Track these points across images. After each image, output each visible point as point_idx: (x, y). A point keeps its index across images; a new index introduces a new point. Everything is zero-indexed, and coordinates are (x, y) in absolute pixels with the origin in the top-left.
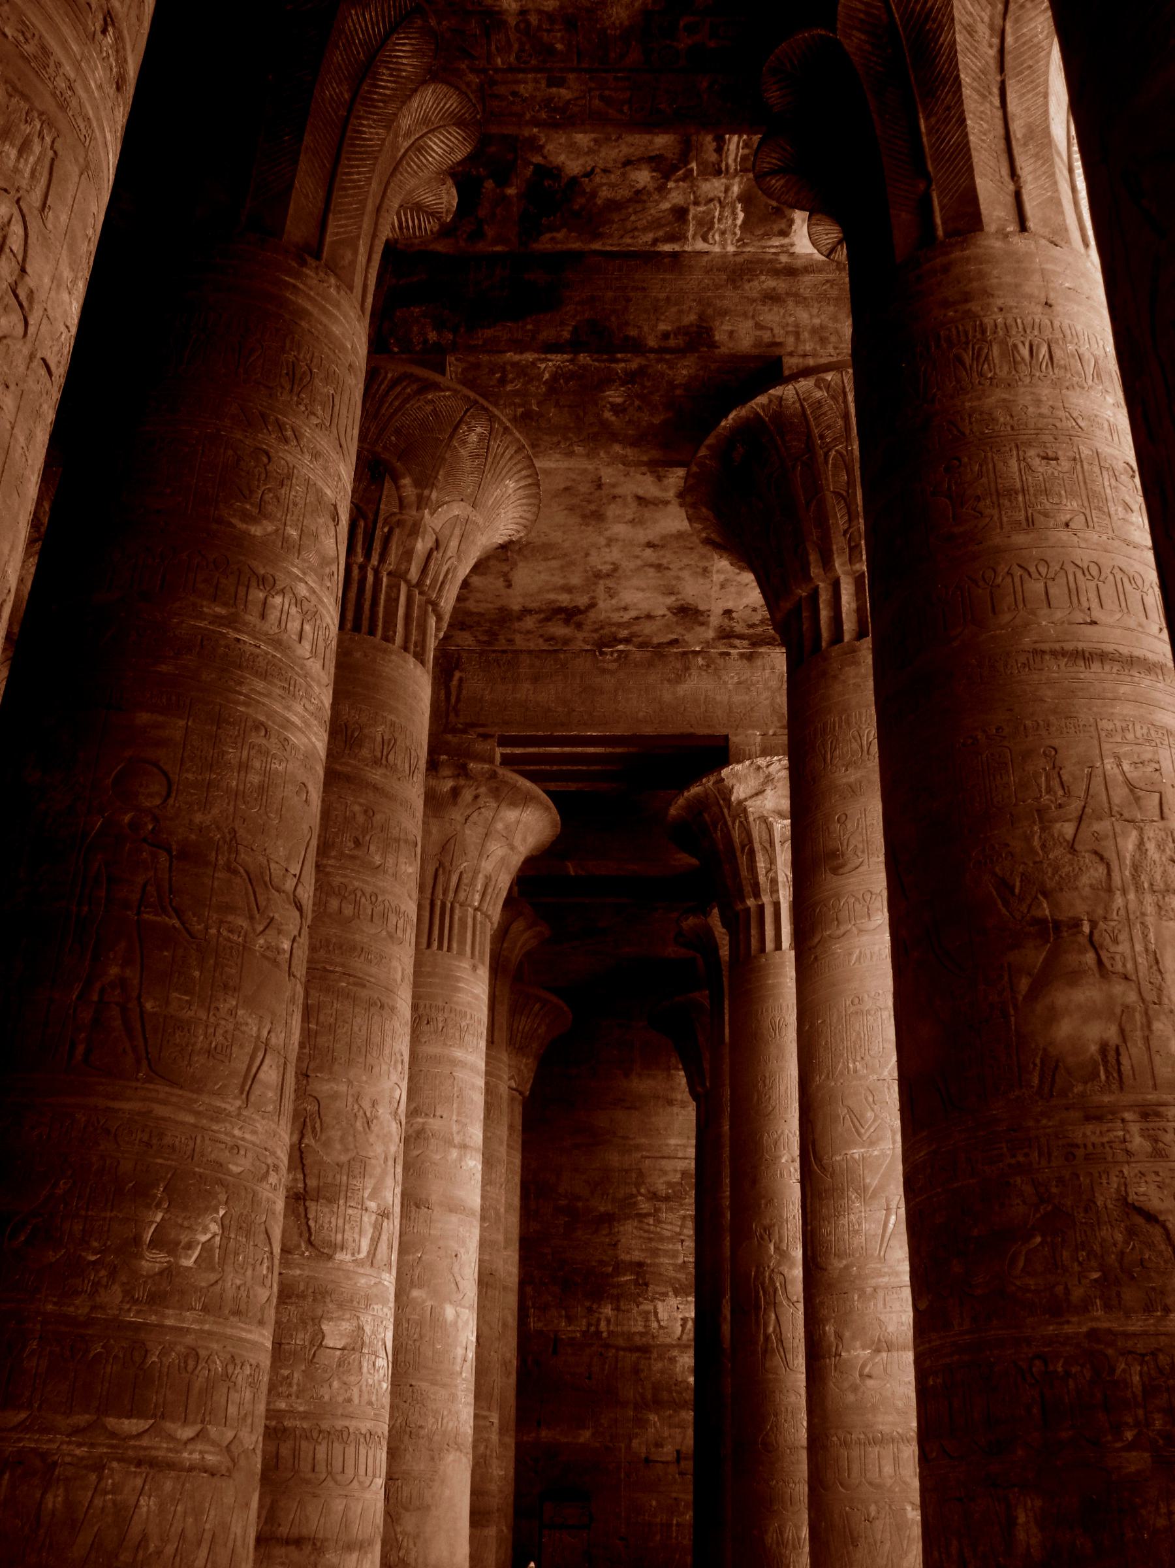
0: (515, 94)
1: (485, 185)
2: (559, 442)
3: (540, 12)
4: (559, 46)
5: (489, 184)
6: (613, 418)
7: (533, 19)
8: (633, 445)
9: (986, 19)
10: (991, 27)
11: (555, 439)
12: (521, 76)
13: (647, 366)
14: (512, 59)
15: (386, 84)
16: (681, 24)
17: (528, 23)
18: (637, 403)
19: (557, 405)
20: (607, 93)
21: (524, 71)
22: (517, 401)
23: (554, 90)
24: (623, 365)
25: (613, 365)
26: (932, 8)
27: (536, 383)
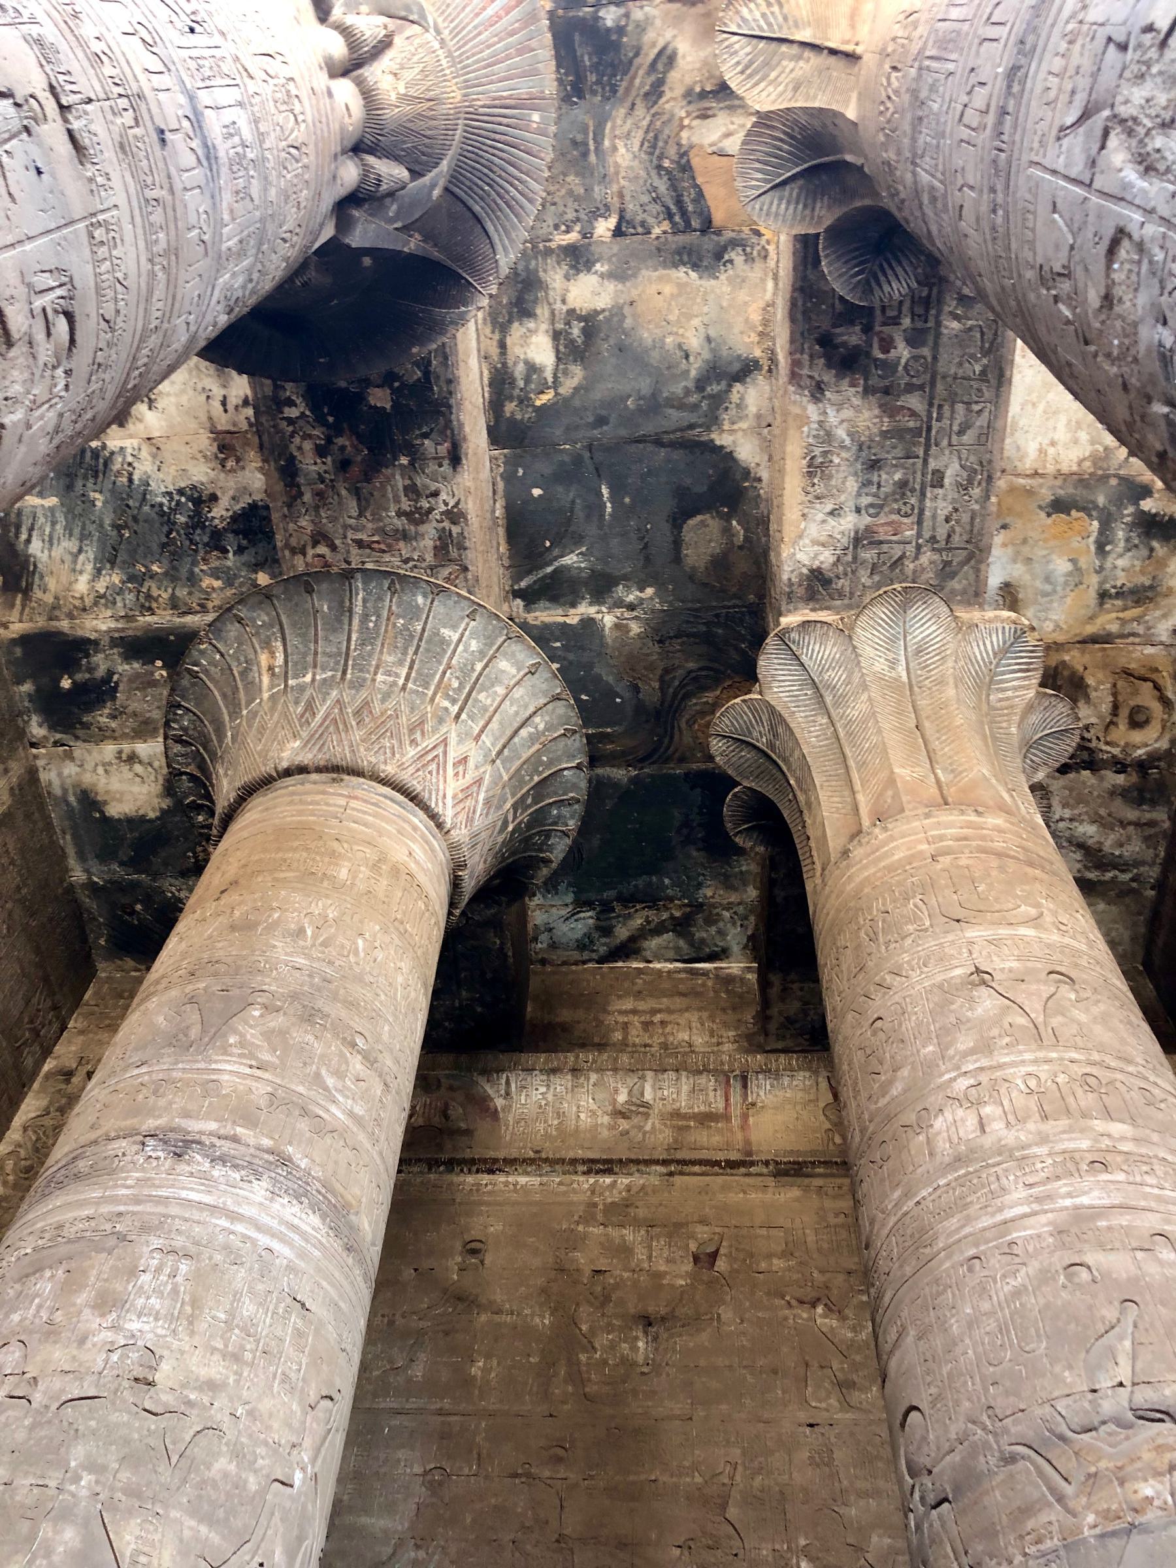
0: (947, 520)
1: (1146, 509)
3: (859, 495)
5: (1147, 505)
7: (865, 501)
9: (792, 65)
10: (799, 58)
12: (927, 513)
14: (905, 520)
15: (835, 676)
16: (881, 356)
17: (871, 505)
20: (956, 428)
21: (922, 511)
23: (947, 481)
26: (785, 133)
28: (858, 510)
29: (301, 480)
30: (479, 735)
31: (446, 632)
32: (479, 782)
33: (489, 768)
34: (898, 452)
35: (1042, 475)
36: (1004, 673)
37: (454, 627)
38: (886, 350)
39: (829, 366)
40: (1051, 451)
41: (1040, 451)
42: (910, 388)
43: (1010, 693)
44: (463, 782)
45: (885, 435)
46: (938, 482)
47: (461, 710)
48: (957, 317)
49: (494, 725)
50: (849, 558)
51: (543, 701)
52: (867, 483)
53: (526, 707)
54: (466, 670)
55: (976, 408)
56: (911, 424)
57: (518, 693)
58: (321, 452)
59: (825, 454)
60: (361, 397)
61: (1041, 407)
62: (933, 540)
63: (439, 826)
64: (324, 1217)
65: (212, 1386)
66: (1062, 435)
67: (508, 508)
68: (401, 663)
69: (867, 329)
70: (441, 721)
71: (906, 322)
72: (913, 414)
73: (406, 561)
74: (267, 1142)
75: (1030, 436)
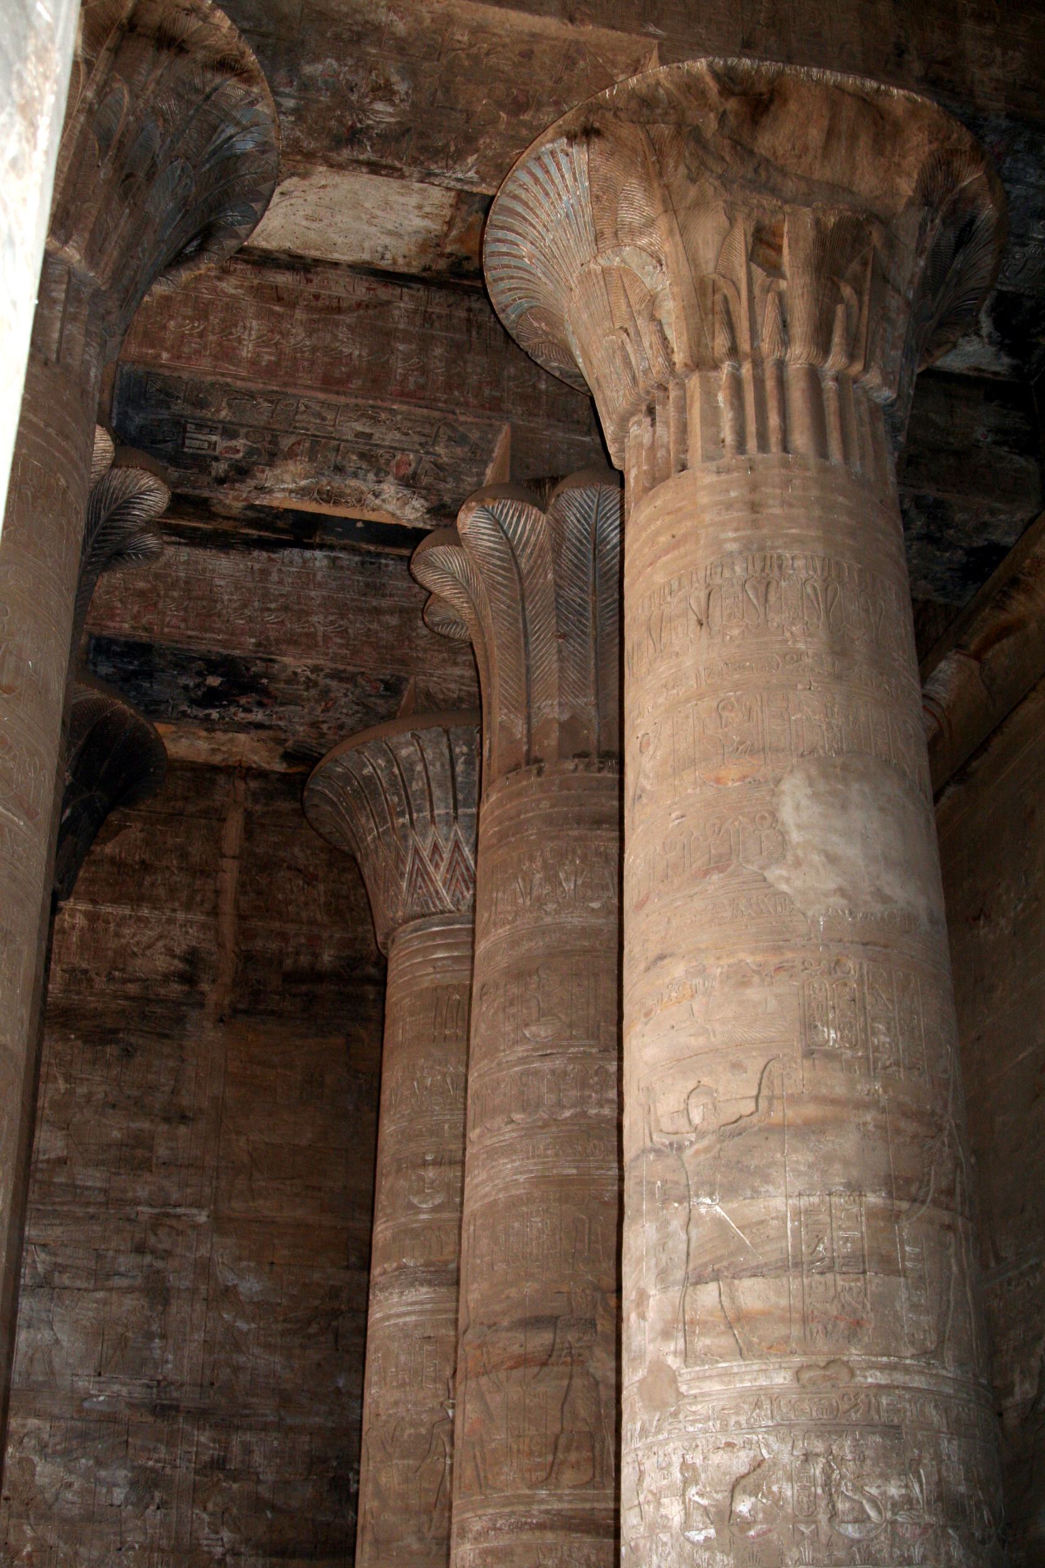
0: (407, 434)
2: (487, 54)
4: (354, 457)
6: (395, 78)
7: (371, 476)
8: (378, 28)
11: (493, 60)
13: (331, 150)
14: (399, 457)
17: (377, 475)
18: (354, 97)
19: (469, 115)
22: (524, 132)
23: (368, 430)
24: (361, 157)
25: (374, 158)
27: (490, 153)
28: (380, 482)
29: (267, 723)
30: (432, 816)
31: (365, 772)
32: (457, 846)
33: (456, 827)
34: (332, 456)
35: (453, 218)
36: (515, 531)
37: (365, 766)
38: (238, 451)
39: (243, 482)
40: (427, 209)
41: (424, 217)
42: (274, 441)
43: (533, 539)
44: (443, 866)
45: (311, 460)
46: (370, 436)
47: (411, 814)
48: (218, 411)
49: (437, 793)
50: (424, 492)
51: (445, 740)
52: (355, 475)
53: (442, 754)
54: (393, 783)
55: (303, 408)
56: (307, 445)
57: (429, 755)
58: (248, 710)
59: (319, 492)
60: (211, 689)
61: (379, 213)
62: (420, 444)
63: (450, 912)
64: (430, 1283)
65: (396, 1403)
66: (413, 200)
67: (369, 542)
68: (368, 820)
69: (216, 459)
70: (405, 838)
71: (214, 438)
72: (298, 443)
73: (346, 695)
74: (395, 1265)
75: (406, 222)
